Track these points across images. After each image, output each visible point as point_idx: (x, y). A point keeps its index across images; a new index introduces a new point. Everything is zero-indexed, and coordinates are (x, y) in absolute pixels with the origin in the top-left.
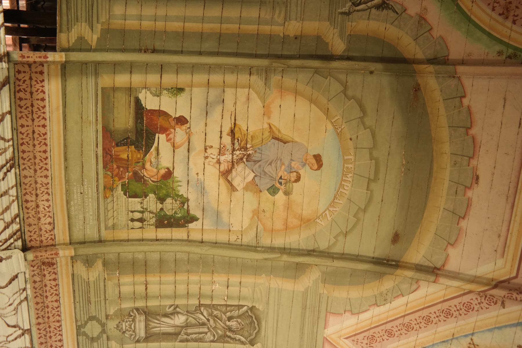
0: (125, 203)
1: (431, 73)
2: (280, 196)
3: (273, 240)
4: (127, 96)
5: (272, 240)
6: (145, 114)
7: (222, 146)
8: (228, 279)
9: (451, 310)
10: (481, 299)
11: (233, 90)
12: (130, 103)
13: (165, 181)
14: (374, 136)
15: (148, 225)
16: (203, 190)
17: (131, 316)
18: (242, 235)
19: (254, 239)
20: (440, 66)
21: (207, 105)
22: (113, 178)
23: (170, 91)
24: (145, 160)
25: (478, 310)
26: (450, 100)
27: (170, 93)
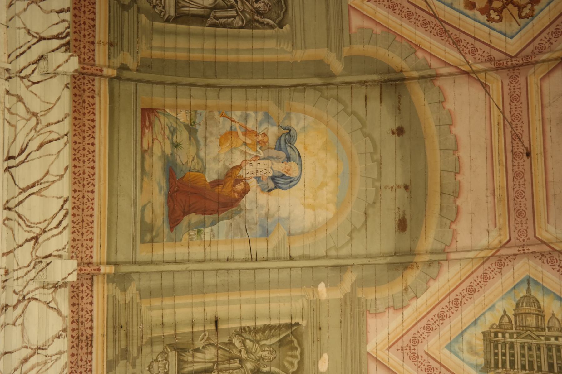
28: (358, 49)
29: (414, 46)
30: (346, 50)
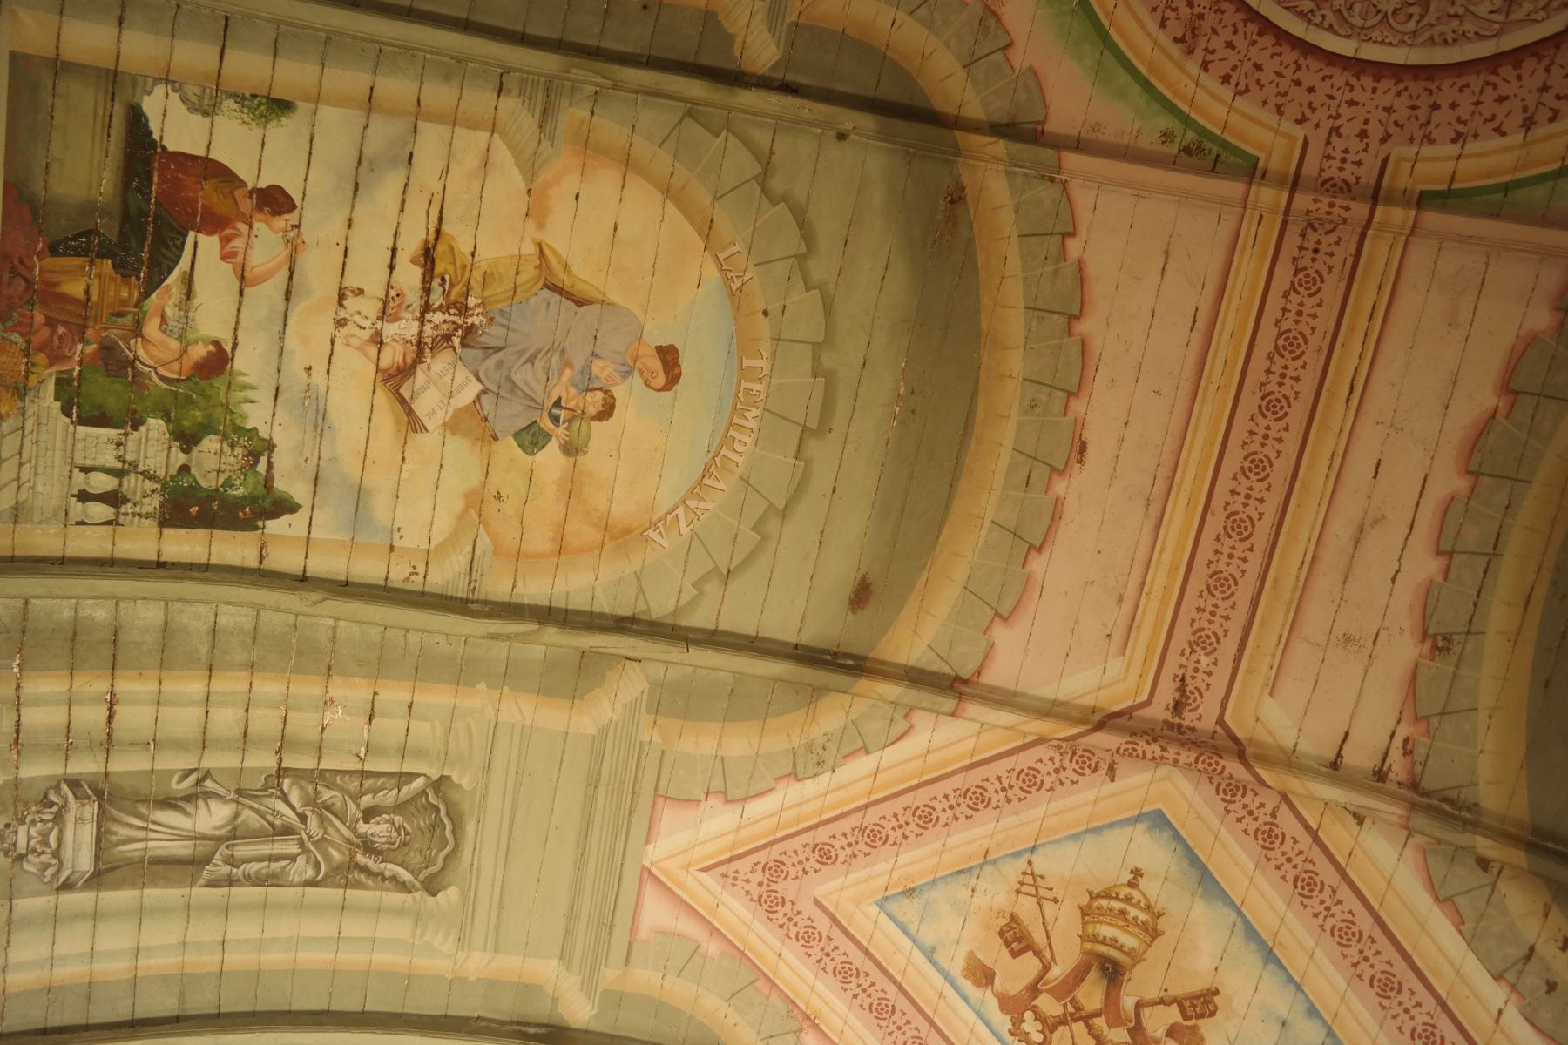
0: (65, 441)
1: (997, 159)
2: (551, 455)
3: (519, 584)
4: (101, 99)
5: (515, 581)
6: (156, 165)
7: (392, 293)
8: (375, 694)
9: (986, 791)
10: (1061, 760)
11: (443, 130)
12: (110, 120)
13: (203, 382)
14: (828, 309)
15: (134, 514)
16: (320, 421)
17: (52, 804)
18: (427, 563)
19: (462, 576)
20: (1022, 146)
21: (359, 163)
22: (27, 355)
23: (246, 103)
24: (145, 308)
25: (1052, 789)
26: (1035, 239)
27: (246, 110)
28: (644, 978)
29: (801, 1019)
30: (610, 975)
